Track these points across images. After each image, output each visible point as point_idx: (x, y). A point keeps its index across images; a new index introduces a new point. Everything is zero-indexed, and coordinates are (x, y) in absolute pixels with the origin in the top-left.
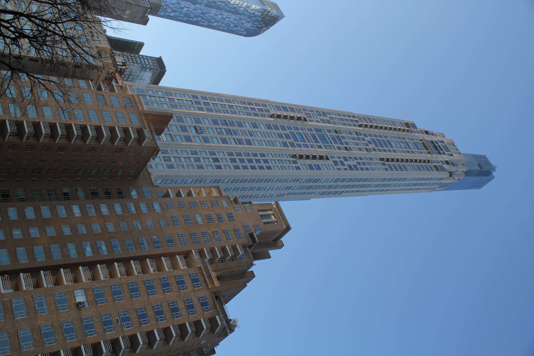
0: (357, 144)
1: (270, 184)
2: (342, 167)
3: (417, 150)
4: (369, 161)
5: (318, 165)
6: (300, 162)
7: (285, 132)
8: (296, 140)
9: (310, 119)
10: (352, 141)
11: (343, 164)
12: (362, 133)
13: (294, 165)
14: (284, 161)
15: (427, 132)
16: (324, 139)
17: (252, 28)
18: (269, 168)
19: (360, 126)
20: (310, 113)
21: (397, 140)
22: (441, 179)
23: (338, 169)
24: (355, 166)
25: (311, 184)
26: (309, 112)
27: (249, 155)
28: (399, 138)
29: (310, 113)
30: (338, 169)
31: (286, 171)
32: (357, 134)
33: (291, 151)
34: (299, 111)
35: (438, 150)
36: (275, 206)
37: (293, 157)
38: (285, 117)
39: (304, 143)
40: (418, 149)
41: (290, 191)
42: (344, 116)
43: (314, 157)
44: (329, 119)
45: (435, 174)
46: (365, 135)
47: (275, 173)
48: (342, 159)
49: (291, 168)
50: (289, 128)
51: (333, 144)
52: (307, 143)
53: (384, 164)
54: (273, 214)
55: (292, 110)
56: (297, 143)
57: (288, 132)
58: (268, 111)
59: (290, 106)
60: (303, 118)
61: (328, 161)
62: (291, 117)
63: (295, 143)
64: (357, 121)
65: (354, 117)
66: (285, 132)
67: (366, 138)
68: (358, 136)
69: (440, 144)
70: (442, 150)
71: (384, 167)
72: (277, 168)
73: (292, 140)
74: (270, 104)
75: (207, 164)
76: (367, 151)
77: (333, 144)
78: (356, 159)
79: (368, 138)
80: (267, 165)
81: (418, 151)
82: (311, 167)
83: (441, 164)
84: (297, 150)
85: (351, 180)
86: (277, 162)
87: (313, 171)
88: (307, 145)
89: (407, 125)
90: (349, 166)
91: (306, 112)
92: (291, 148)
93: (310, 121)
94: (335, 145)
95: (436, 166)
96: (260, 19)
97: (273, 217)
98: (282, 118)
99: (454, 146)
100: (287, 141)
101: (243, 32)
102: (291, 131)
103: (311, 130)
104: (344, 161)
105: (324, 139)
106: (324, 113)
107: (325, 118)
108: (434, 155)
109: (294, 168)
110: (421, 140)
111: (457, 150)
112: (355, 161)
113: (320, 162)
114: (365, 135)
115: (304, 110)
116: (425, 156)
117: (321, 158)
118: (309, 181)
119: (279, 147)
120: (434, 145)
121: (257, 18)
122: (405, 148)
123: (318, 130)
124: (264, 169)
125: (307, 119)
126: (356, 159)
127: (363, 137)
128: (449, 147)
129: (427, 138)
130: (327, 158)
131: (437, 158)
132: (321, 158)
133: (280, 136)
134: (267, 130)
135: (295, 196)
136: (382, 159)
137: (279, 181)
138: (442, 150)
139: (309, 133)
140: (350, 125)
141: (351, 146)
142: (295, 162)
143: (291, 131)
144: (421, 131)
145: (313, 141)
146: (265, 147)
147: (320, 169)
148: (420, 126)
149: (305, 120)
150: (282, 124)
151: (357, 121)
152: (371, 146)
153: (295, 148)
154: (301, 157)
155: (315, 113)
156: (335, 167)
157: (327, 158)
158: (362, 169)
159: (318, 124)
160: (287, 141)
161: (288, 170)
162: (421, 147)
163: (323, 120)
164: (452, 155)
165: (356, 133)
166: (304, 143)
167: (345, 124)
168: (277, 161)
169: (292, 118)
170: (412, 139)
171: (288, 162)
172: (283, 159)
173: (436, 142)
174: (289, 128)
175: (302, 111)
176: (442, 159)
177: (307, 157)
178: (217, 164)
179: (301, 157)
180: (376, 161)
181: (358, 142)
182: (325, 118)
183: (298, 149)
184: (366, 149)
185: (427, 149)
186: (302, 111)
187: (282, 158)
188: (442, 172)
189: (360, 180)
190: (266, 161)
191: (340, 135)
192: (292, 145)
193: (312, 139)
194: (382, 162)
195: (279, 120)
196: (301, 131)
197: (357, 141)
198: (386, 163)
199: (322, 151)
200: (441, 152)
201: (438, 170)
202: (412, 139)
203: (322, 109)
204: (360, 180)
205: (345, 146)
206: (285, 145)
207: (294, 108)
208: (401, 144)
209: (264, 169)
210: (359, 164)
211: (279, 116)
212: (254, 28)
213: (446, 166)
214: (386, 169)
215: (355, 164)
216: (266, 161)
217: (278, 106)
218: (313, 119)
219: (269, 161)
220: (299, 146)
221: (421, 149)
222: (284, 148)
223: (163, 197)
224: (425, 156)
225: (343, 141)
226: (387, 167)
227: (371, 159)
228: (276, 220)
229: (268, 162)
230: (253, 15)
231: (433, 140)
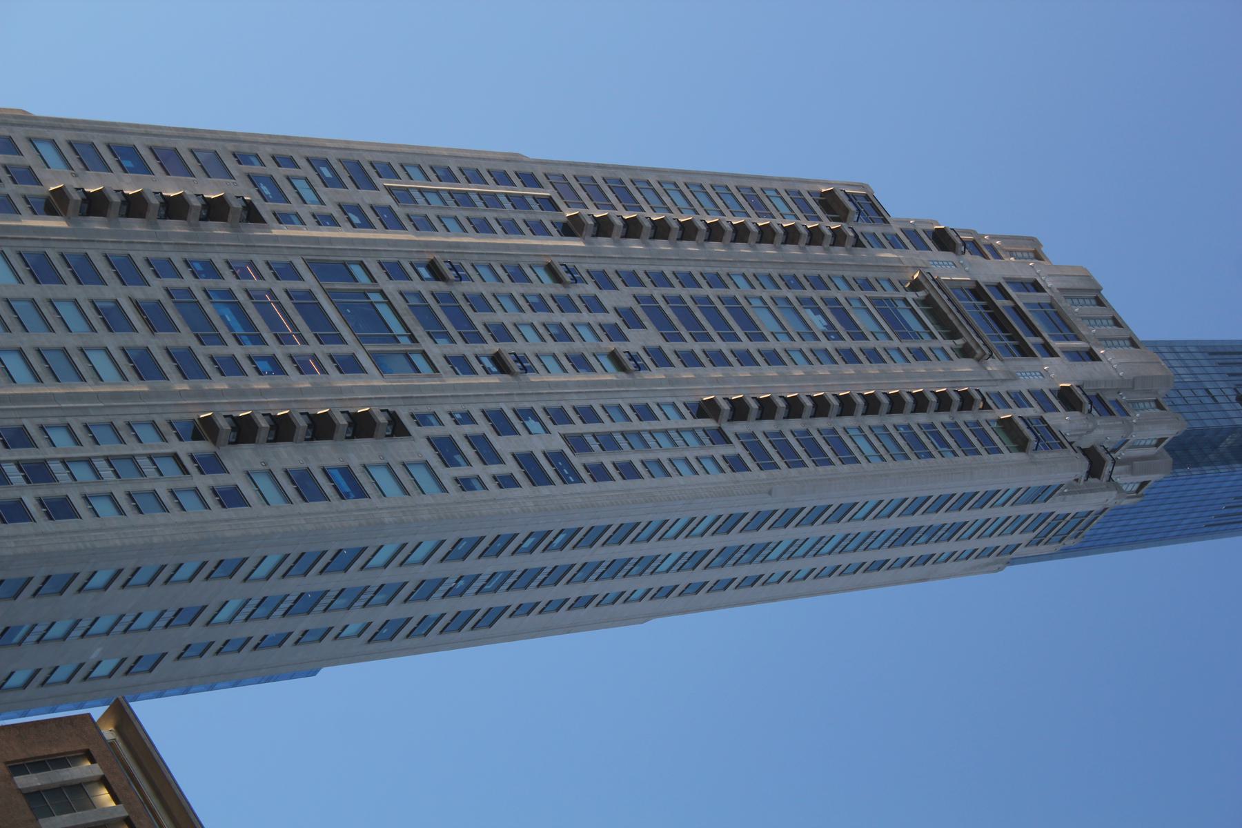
0: (561, 335)
1: (73, 605)
2: (486, 472)
3: (896, 343)
4: (636, 424)
5: (347, 472)
6: (240, 460)
7: (139, 293)
8: (208, 335)
9: (281, 207)
10: (529, 316)
11: (489, 455)
12: (582, 268)
13: (204, 482)
14: (144, 463)
15: (943, 240)
16: (367, 320)
18: (59, 509)
19: (570, 228)
20: (279, 173)
21: (785, 292)
22: (1045, 493)
23: (465, 484)
24: (556, 458)
25: (314, 582)
26: (271, 169)
27: (467, 418)
28: (793, 282)
29: (279, 173)
30: (465, 484)
31: (160, 517)
32: (557, 278)
33: (181, 396)
34: (213, 164)
35: (1014, 336)
36: (108, 732)
37: (196, 436)
38: (134, 206)
39: (255, 350)
40: (903, 336)
41: (196, 633)
42: (475, 176)
43: (321, 428)
44: (387, 200)
45: (1008, 470)
46: (603, 280)
47: (102, 532)
48: (483, 427)
49: (188, 500)
50: (163, 268)
51: (426, 343)
52: (273, 347)
53: (720, 437)
54: (104, 781)
55: (170, 160)
56: (217, 350)
57: (155, 290)
58: (29, 176)
59: (157, 142)
60: (236, 205)
61: (401, 444)
62: (167, 201)
63: (202, 353)
64: (549, 204)
65: (529, 180)
66: (139, 293)
67: (607, 298)
68: (559, 290)
69: (1022, 299)
70: (1036, 333)
71: (720, 451)
72: (104, 507)
73: (185, 338)
74: (34, 133)
76: (621, 367)
77: (426, 343)
78: (559, 416)
80: (45, 491)
81: (904, 345)
82: (305, 485)
83: (1033, 411)
84: (222, 393)
85: (540, 539)
86: (106, 472)
87: (320, 506)
88: (273, 360)
89: (830, 203)
90: (526, 461)
91: (256, 169)
92: (184, 386)
93: (282, 219)
94: (437, 350)
95: (1007, 426)
97: (104, 797)
98: (113, 211)
99: (1100, 302)
100: (156, 344)
102: (173, 282)
103: (286, 271)
104: (492, 436)
105: (367, 320)
106: (355, 168)
107: (364, 198)
108: (993, 366)
109: (210, 499)
110: (915, 286)
111: (1117, 322)
112: (557, 430)
113: (358, 454)
114: (603, 280)
115: (241, 158)
116: (947, 372)
117: (361, 426)
118: (302, 563)
119: (111, 384)
120: (990, 306)
122: (831, 333)
123: (331, 268)
124: (26, 516)
125: (265, 209)
126: (559, 416)
127: (590, 288)
128: (1075, 311)
129: (950, 269)
131: (1014, 378)
132: (361, 426)
133: (112, 318)
134: (31, 289)
135: (230, 660)
136: (705, 409)
137: (123, 579)
138: (1036, 333)
139: (279, 287)
140: (511, 228)
141: (526, 346)
142: (210, 465)
143: (173, 282)
144: (912, 235)
145: (308, 335)
146: (25, 386)
147: (361, 493)
148: (905, 205)
149: (252, 214)
150: (116, 250)
151: (549, 204)
152: (639, 340)
153: (205, 385)
154: (244, 430)
155: (306, 170)
156: (447, 474)
157: (397, 428)
158: (599, 473)
159: (326, 233)
160: (156, 344)
161: (175, 515)
162: (916, 326)
163: (357, 209)
164: (1092, 356)
165: (550, 269)
166: (255, 350)
167: (483, 227)
168: (101, 465)
169: (174, 208)
170: (866, 285)
171: (168, 466)
172: (138, 450)
173: (999, 287)
174: (163, 268)
175: (231, 164)
176: (1038, 384)
177: (282, 429)
179: (244, 430)
180: (675, 423)
181: (566, 319)
182: (364, 198)
183: (220, 384)
184: (613, 356)
185: (953, 334)
186: (231, 164)
187: (132, 448)
188: (1042, 455)
189: (593, 536)
190: (37, 472)
191: (459, 289)
192: (188, 365)
193: (299, 320)
194: (709, 423)
195: (96, 224)
196: (230, 282)
197: (558, 317)
199: (368, 389)
200: (1031, 340)
201: (1021, 444)
202: (866, 285)
203: (347, 147)
204: (593, 536)
205: (492, 347)
206: (144, 365)
207: (183, 147)
208: (808, 314)
209: (26, 516)
210: (578, 444)
211: (95, 204)
213: (1062, 420)
214: (736, 464)
216: (37, 472)
217: (88, 144)
218: (295, 206)
219: (56, 467)
220: (229, 366)
221: (917, 336)
222: (143, 387)
224: (947, 372)
225: (478, 319)
226: (737, 449)
227: (644, 413)
228: (122, 812)
229: (50, 478)
231: (983, 279)
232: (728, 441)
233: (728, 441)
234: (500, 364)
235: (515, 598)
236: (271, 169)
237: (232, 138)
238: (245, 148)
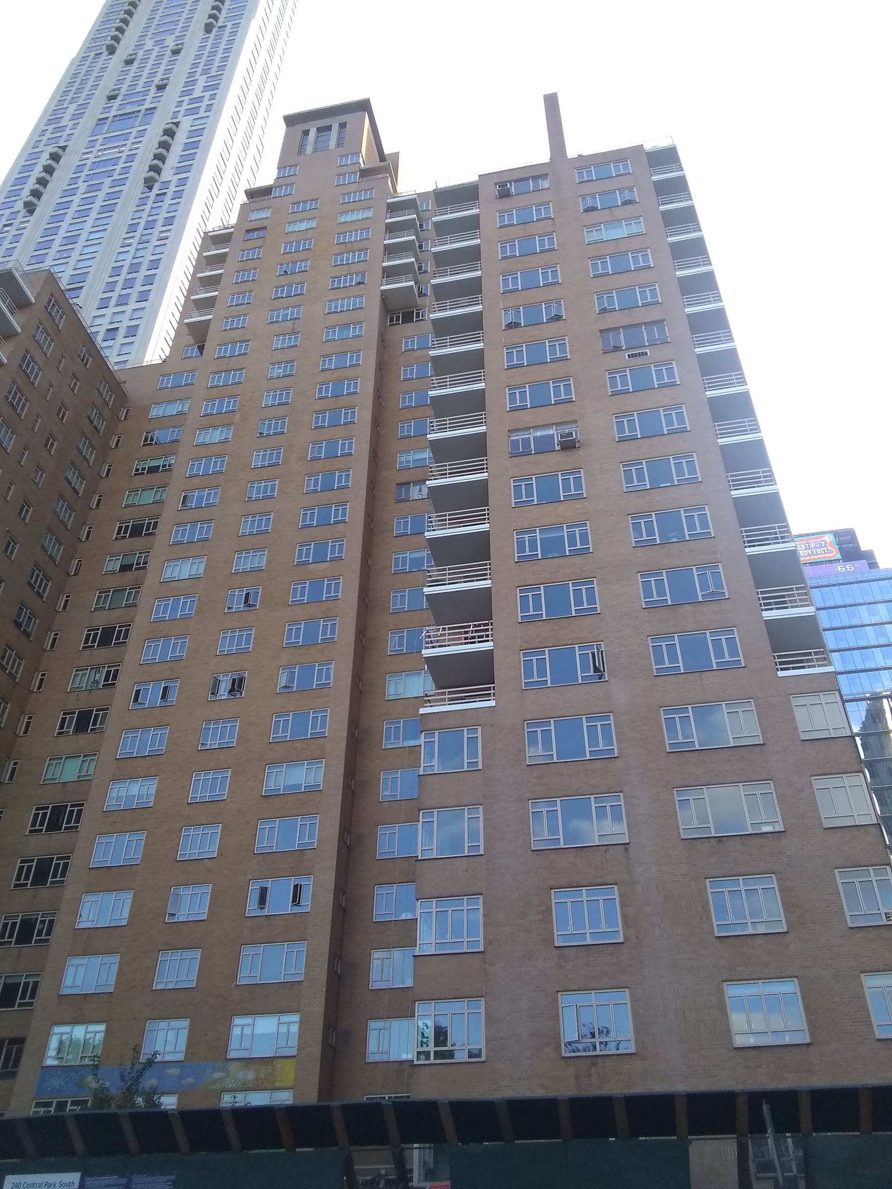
6: (167, 174)
11: (200, 99)
13: (173, 188)
20: (48, 135)
26: (45, 138)
29: (48, 135)
33: (133, 188)
37: (150, 188)
39: (122, 160)
43: (165, 145)
46: (139, 46)
51: (143, 108)
57: (83, 187)
63: (116, 176)
71: (228, 29)
73: (108, 182)
75: (116, 352)
77: (143, 108)
79: (149, 44)
90: (206, 89)
100: (106, 189)
113: (181, 138)
125: (62, 144)
132: (170, 133)
136: (208, 28)
143: (81, 180)
156: (202, 114)
157: (177, 124)
160: (106, 189)
178: (122, 332)
180: (211, 41)
191: (123, 91)
192: (121, 182)
194: (215, 30)
198: (220, 23)
199: (154, 133)
205: (153, 89)
210: (205, 72)
215: (204, 78)
220: (126, 170)
223: (201, 349)
225: (139, 89)
232: (225, 26)
233: (225, 26)
234: (161, 88)
235: (257, 131)
236: (45, 138)
238: (32, 144)
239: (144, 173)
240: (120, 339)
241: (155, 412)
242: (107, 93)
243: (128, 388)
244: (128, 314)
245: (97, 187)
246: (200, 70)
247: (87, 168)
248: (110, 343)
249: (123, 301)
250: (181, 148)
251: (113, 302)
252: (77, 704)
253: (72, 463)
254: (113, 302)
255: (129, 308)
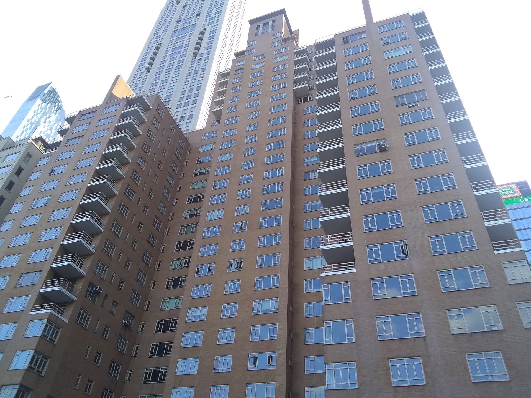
2: (216, 19)
6: (202, 50)
7: (168, 61)
8: (179, 53)
13: (204, 56)
17: (57, 115)
26: (153, 41)
33: (189, 58)
37: (196, 57)
39: (184, 46)
43: (201, 39)
48: (208, 18)
51: (191, 24)
56: (182, 52)
57: (168, 59)
63: (182, 54)
66: (168, 61)
73: (178, 56)
75: (184, 126)
77: (191, 24)
90: (216, 13)
96: (49, 105)
100: (178, 59)
101: (58, 125)
113: (207, 35)
121: (48, 107)
130: (205, 29)
132: (202, 33)
154: (197, 49)
155: (155, 37)
156: (215, 24)
157: (205, 29)
160: (178, 59)
177: (199, 44)
178: (187, 118)
191: (183, 18)
192: (184, 56)
199: (196, 34)
205: (195, 16)
210: (215, 6)
212: (57, 114)
220: (185, 51)
223: (219, 121)
225: (189, 17)
230: (44, 110)
234: (198, 15)
235: (238, 28)
236: (153, 41)
237: (145, 46)
239: (193, 51)
240: (186, 120)
241: (201, 149)
242: (177, 20)
243: (190, 140)
244: (189, 110)
245: (174, 59)
246: (213, 6)
247: (170, 51)
248: (182, 122)
249: (186, 105)
250: (207, 39)
251: (183, 105)
252: (174, 275)
253: (169, 173)
254: (183, 105)
255: (189, 108)
